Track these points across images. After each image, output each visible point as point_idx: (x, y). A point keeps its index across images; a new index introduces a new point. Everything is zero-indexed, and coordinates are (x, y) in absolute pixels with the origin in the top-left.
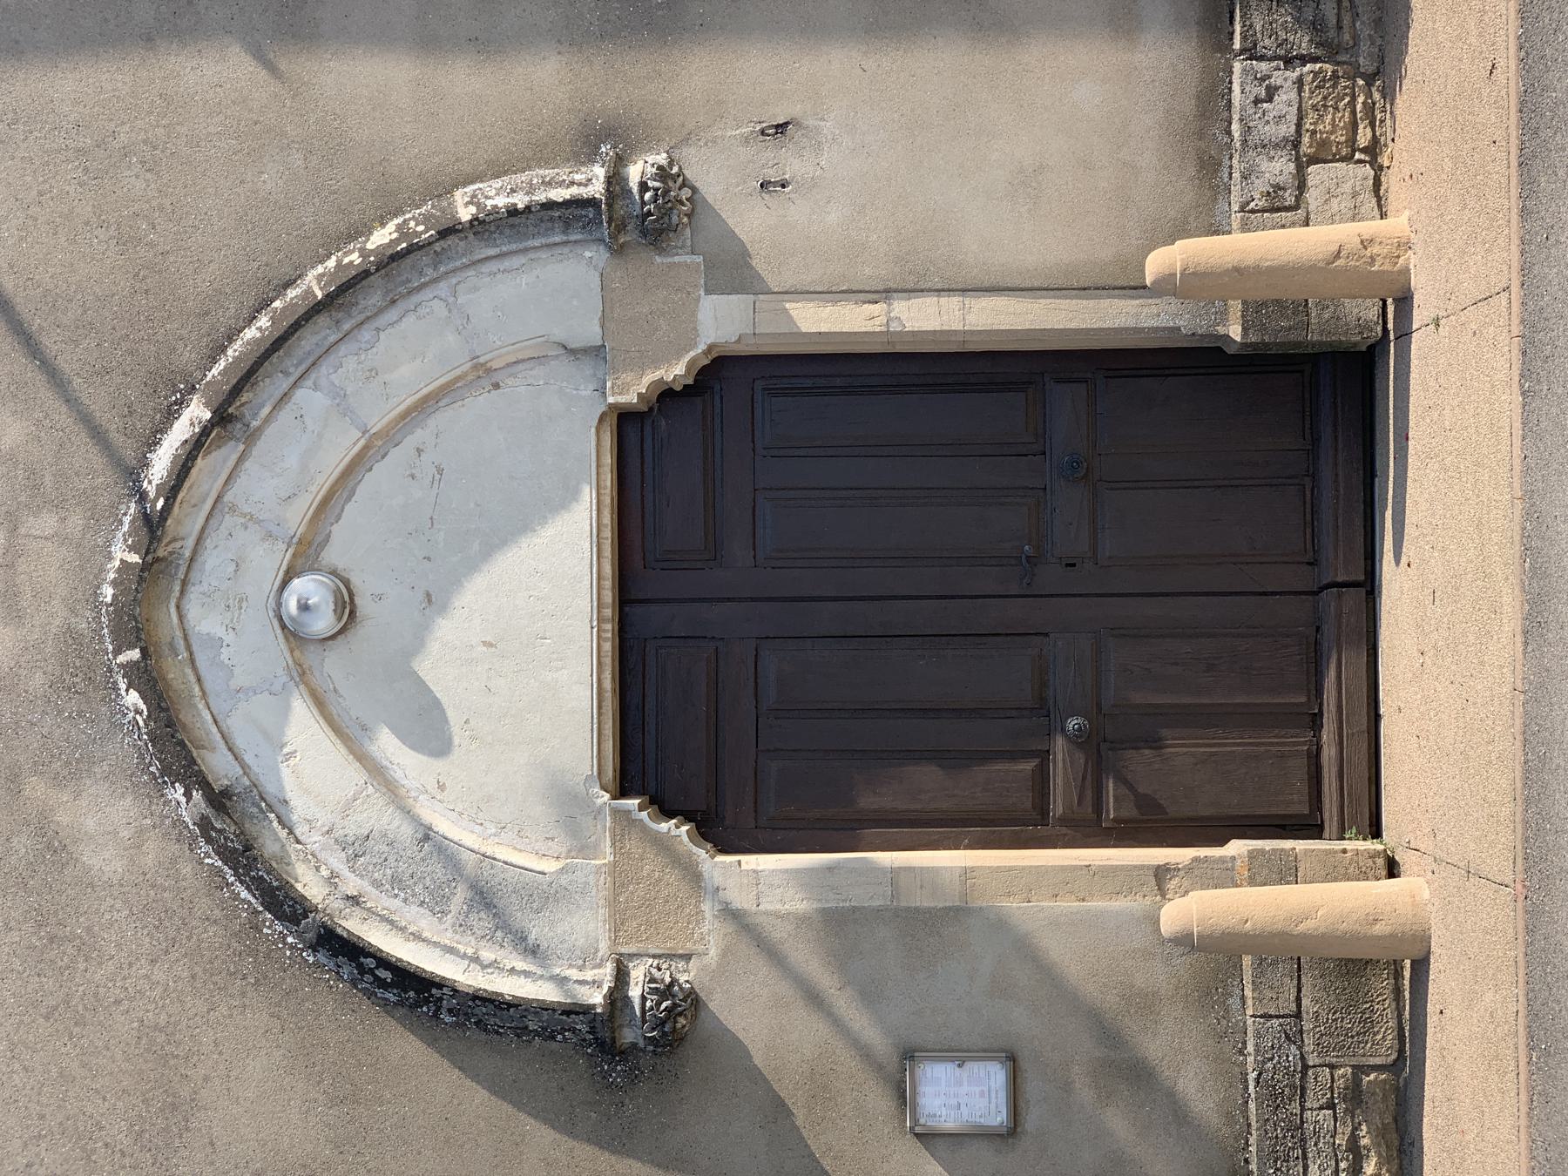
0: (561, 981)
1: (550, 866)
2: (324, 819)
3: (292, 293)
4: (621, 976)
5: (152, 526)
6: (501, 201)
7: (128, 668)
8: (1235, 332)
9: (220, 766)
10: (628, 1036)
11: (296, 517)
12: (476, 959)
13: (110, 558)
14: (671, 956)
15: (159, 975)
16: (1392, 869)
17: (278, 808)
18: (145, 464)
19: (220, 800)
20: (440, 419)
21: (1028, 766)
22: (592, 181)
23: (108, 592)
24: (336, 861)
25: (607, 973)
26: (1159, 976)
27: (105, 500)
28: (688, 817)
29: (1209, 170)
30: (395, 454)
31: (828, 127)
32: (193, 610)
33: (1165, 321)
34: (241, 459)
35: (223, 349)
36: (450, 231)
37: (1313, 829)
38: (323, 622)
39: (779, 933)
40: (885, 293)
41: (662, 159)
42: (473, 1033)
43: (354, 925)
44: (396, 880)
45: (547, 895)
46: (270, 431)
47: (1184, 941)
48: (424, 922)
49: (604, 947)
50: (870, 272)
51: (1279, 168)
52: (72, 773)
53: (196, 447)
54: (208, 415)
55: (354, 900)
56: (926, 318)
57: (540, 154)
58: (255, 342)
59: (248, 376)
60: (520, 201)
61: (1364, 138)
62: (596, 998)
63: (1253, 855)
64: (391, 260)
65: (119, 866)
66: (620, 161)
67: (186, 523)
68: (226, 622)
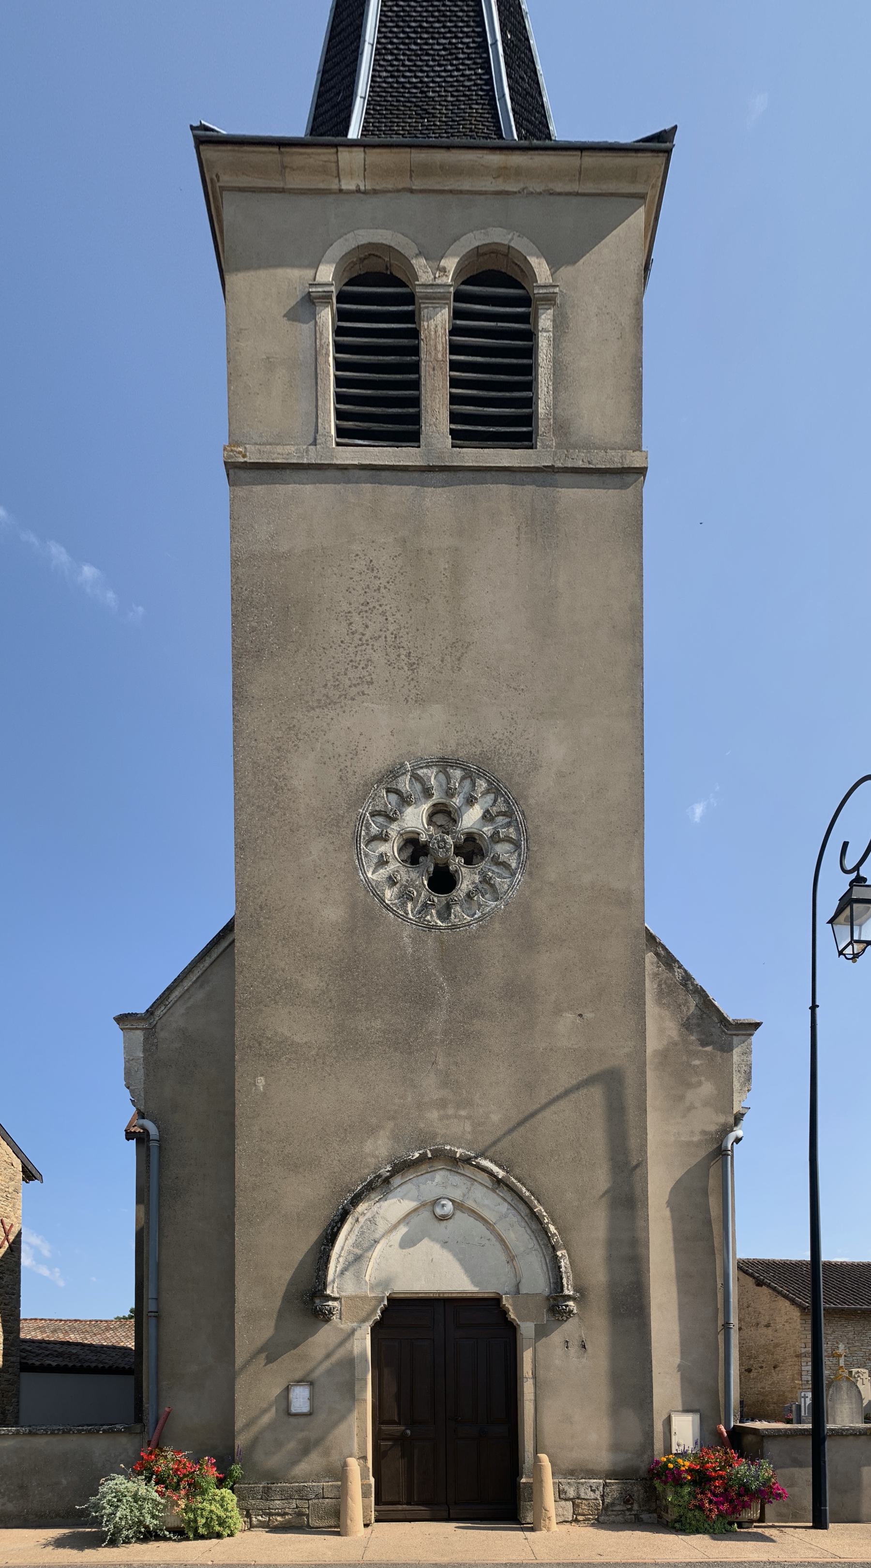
0: (333, 1281)
1: (367, 1278)
2: (381, 1212)
3: (536, 1202)
4: (335, 1299)
5: (467, 1160)
6: (563, 1264)
7: (425, 1154)
8: (523, 1480)
9: (396, 1181)
10: (317, 1301)
11: (470, 1203)
12: (340, 1256)
13: (458, 1148)
14: (341, 1313)
15: (335, 1162)
16: (366, 1525)
17: (384, 1198)
18: (486, 1158)
19: (387, 1181)
20: (498, 1246)
21: (396, 1419)
22: (568, 1291)
23: (448, 1147)
24: (369, 1215)
25: (336, 1295)
26: (335, 1457)
28: (381, 1319)
29: (571, 1473)
30: (488, 1233)
31: (584, 1360)
32: (442, 1173)
33: (527, 1459)
34: (487, 1187)
36: (554, 1249)
37: (376, 1504)
38: (439, 1211)
39: (348, 1345)
40: (535, 1377)
41: (575, 1311)
42: (318, 1255)
43: (350, 1220)
44: (363, 1233)
45: (358, 1277)
46: (495, 1195)
47: (345, 1465)
48: (350, 1241)
49: (343, 1294)
50: (541, 1373)
51: (571, 1493)
52: (396, 1137)
53: (490, 1173)
55: (357, 1220)
56: (528, 1389)
57: (577, 1275)
60: (563, 1269)
61: (580, 1518)
62: (328, 1292)
63: (370, 1485)
64: (546, 1231)
65: (367, 1151)
67: (468, 1171)
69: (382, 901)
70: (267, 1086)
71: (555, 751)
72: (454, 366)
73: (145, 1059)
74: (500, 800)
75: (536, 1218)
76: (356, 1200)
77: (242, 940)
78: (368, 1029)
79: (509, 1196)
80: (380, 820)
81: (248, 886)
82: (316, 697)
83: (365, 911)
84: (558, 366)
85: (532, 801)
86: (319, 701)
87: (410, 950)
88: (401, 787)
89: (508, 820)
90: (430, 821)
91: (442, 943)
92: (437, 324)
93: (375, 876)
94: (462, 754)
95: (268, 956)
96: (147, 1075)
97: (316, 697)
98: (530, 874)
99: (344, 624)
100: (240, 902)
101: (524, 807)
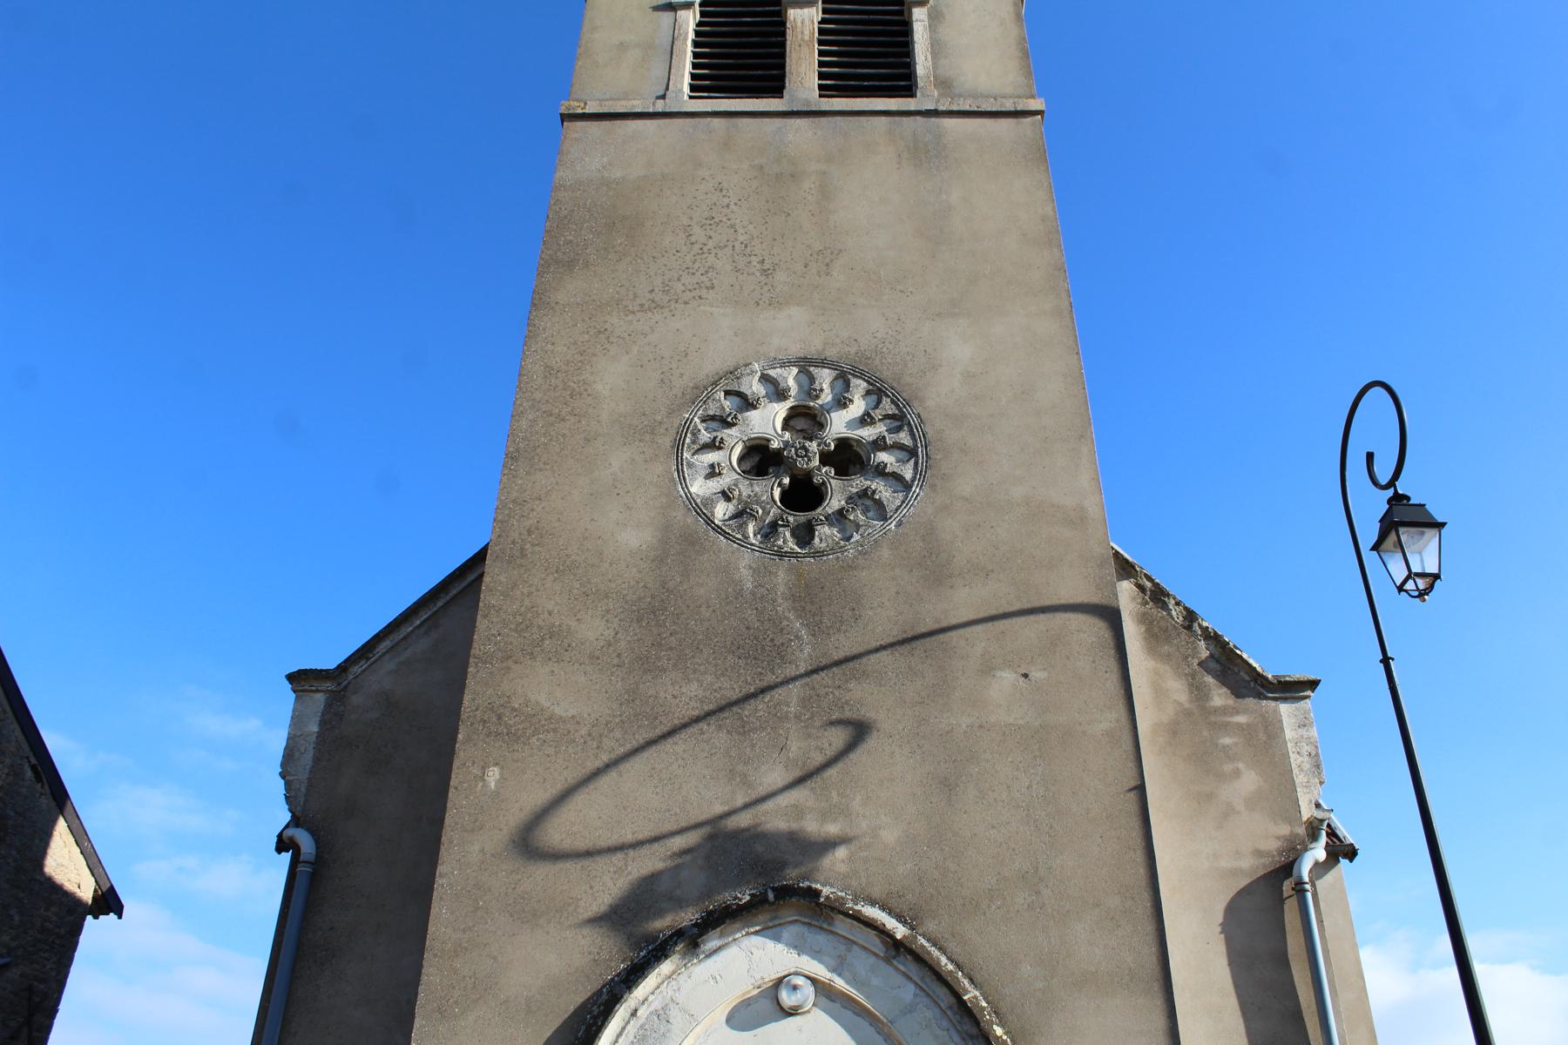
3: (966, 982)
24: (656, 1003)
27: (854, 883)
34: (876, 955)
35: (935, 945)
46: (891, 970)
54: (899, 937)
55: (634, 1013)
58: (939, 962)
59: (920, 959)
67: (842, 926)
69: (709, 521)
70: (503, 778)
71: (958, 349)
73: (319, 734)
74: (886, 402)
75: (966, 1011)
77: (494, 575)
78: (675, 697)
79: (913, 969)
80: (714, 425)
81: (514, 502)
82: (639, 301)
83: (688, 534)
84: (936, 48)
85: (930, 403)
86: (642, 305)
87: (749, 585)
88: (744, 389)
89: (897, 423)
90: (786, 425)
91: (800, 575)
93: (700, 487)
94: (831, 353)
95: (530, 594)
96: (317, 760)
97: (639, 301)
98: (933, 487)
99: (682, 235)
100: (502, 524)
101: (919, 409)
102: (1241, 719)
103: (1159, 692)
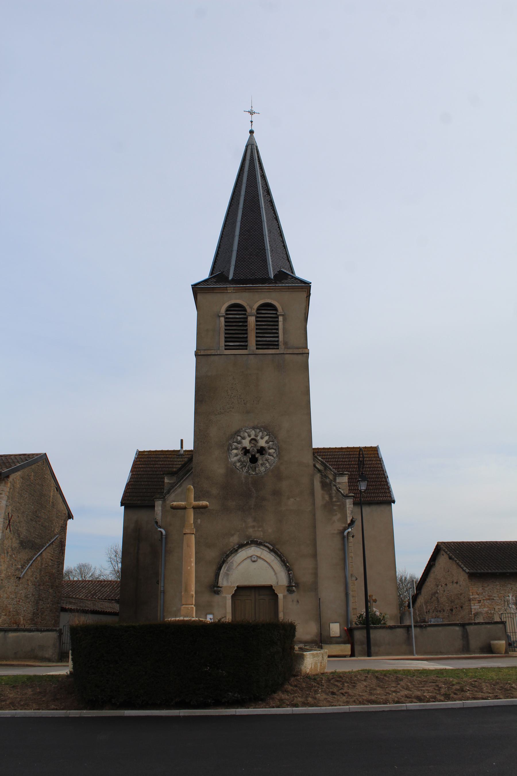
4: (221, 587)
38: (253, 559)
66: (295, 586)
68: (253, 551)
72: (257, 329)
76: (228, 556)
87: (244, 481)
92: (252, 320)
102: (338, 503)
103: (323, 498)
